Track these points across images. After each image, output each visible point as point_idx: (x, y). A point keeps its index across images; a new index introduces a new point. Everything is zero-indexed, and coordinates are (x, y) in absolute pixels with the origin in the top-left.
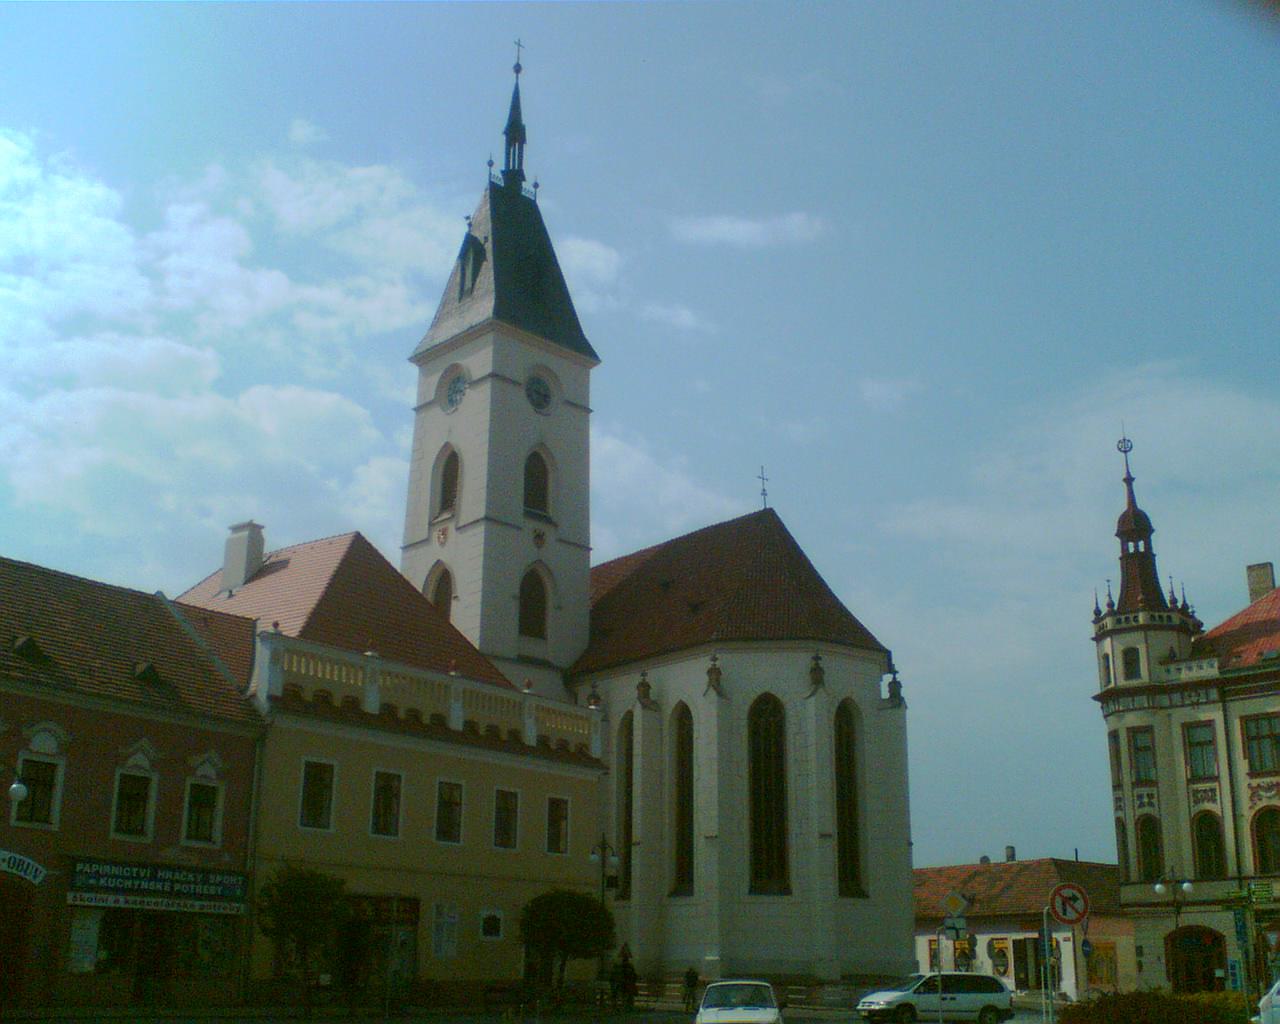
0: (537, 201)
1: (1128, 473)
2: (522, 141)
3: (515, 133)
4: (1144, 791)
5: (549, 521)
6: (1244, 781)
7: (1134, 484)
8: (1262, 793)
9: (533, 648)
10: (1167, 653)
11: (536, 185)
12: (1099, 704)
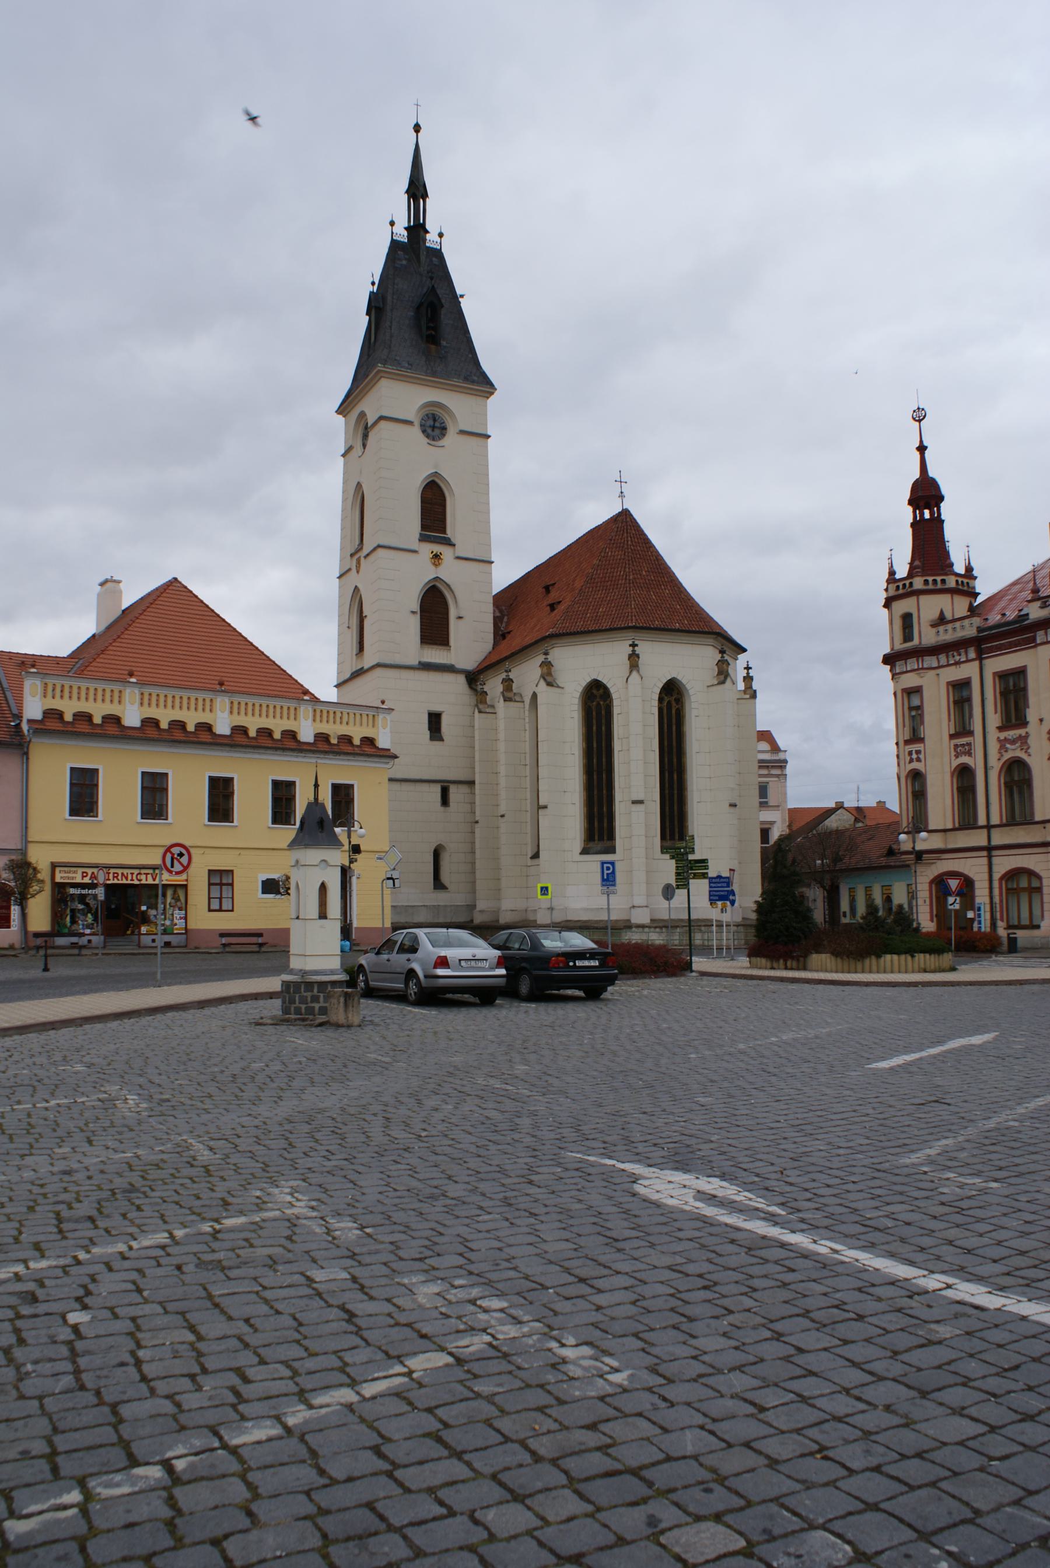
0: (443, 250)
1: (921, 441)
2: (425, 196)
3: (417, 190)
4: (914, 747)
6: (993, 735)
7: (928, 454)
8: (1008, 746)
9: (435, 655)
10: (937, 614)
11: (441, 235)
12: (888, 667)
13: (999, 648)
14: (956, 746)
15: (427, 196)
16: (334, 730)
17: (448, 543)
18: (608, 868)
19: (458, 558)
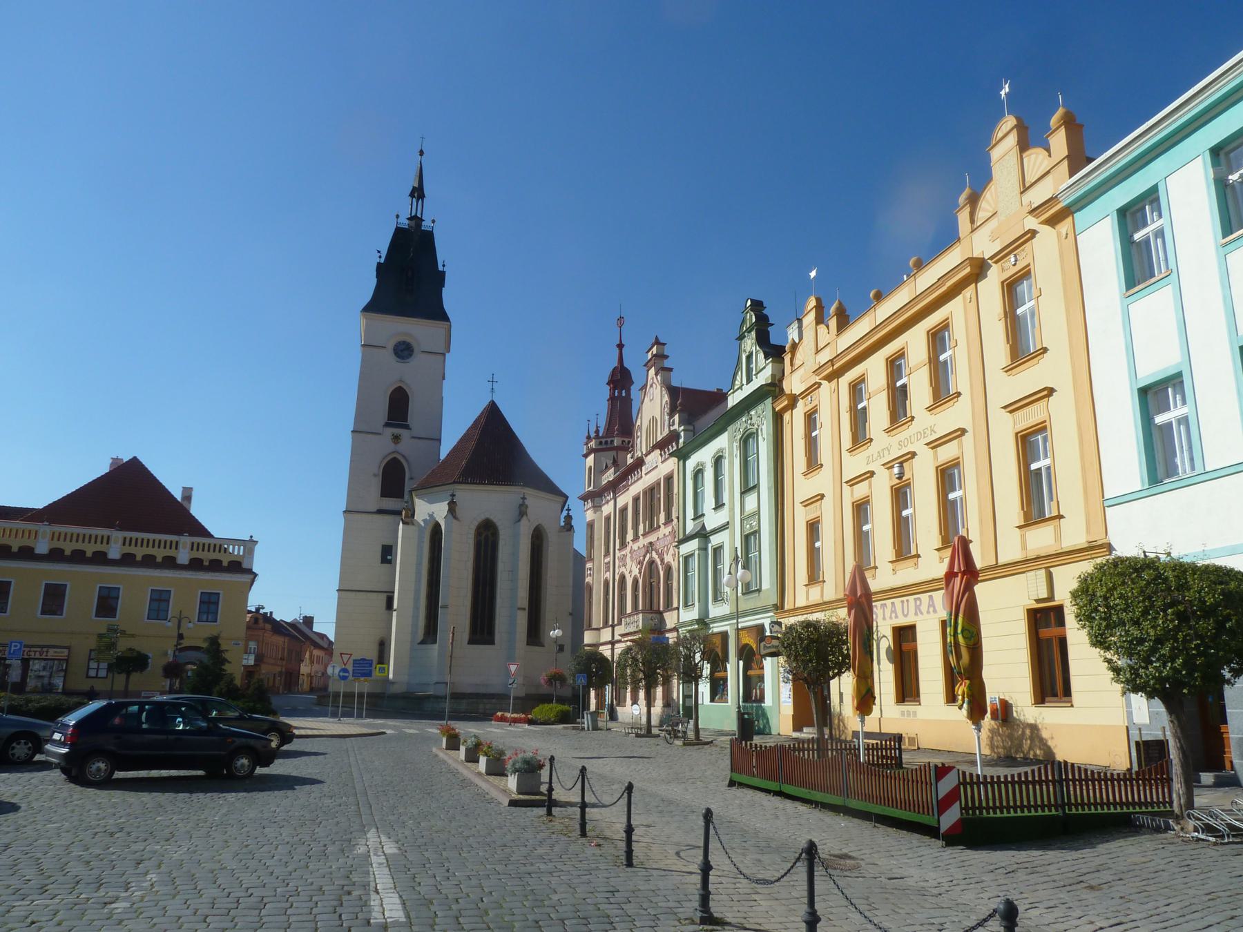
3: (418, 193)
7: (624, 349)
15: (424, 196)
16: (206, 556)
17: (407, 427)
18: (16, 646)
19: (413, 437)
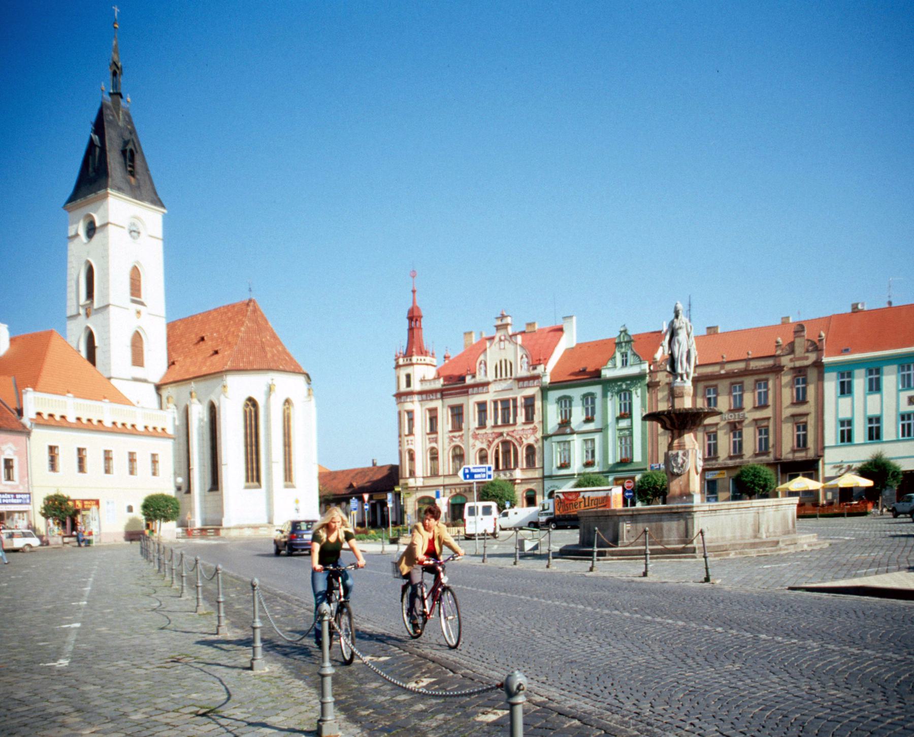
5: (142, 304)
7: (417, 294)
13: (451, 394)
14: (429, 439)
